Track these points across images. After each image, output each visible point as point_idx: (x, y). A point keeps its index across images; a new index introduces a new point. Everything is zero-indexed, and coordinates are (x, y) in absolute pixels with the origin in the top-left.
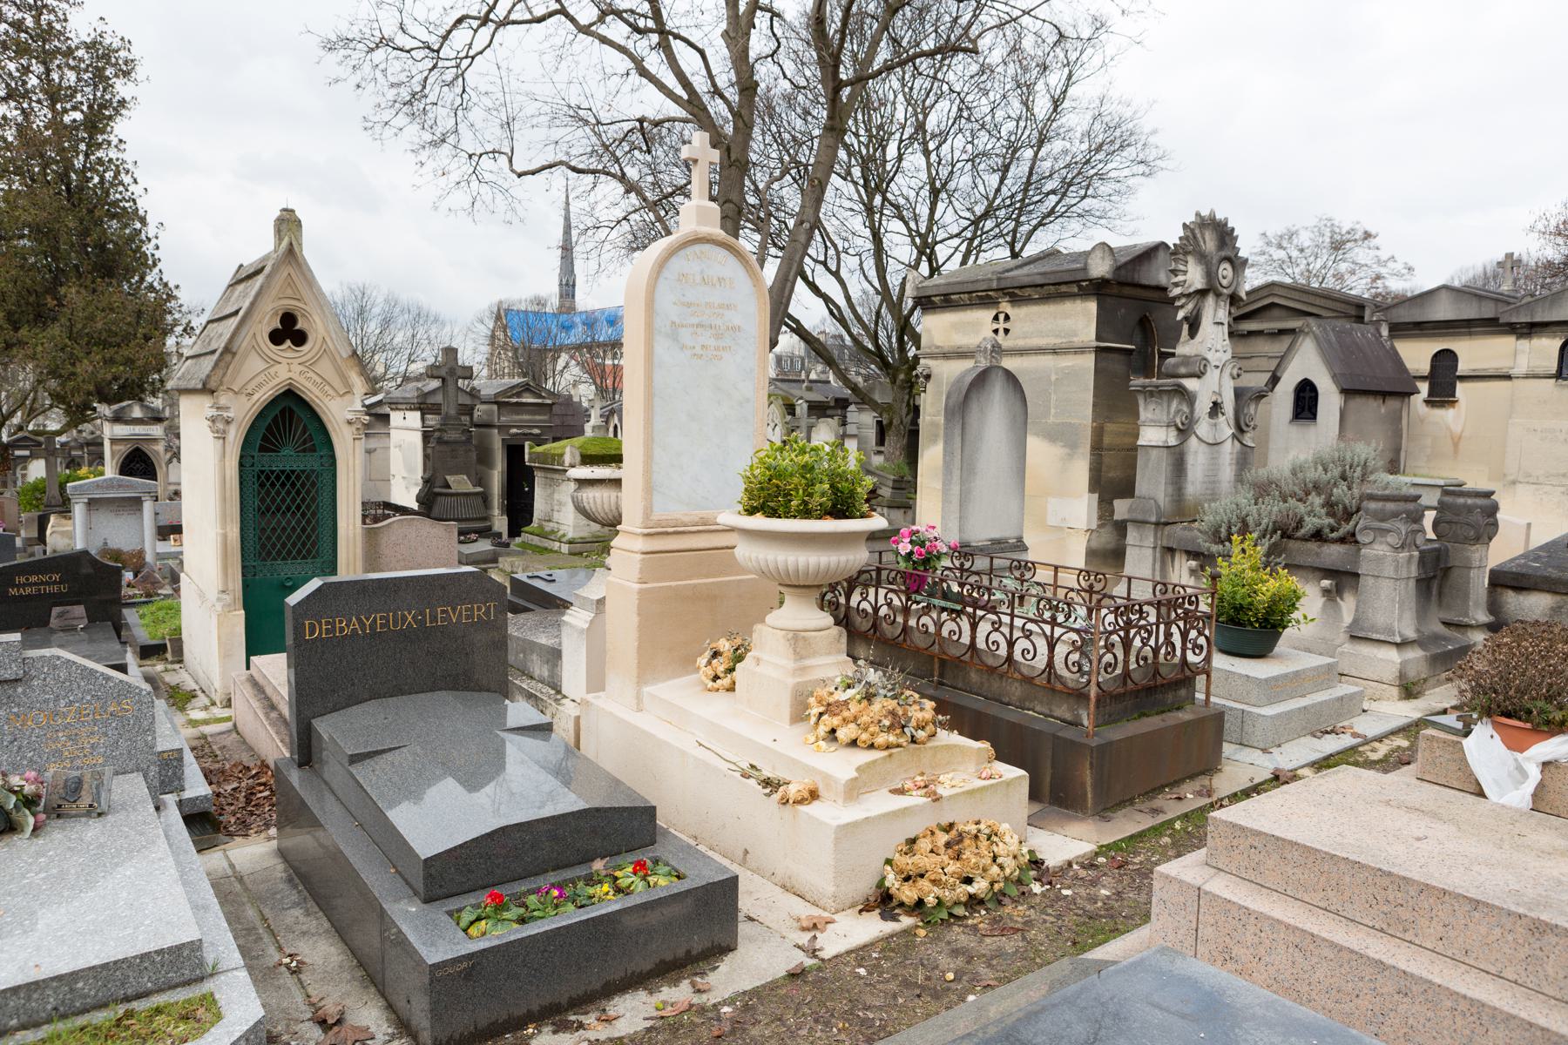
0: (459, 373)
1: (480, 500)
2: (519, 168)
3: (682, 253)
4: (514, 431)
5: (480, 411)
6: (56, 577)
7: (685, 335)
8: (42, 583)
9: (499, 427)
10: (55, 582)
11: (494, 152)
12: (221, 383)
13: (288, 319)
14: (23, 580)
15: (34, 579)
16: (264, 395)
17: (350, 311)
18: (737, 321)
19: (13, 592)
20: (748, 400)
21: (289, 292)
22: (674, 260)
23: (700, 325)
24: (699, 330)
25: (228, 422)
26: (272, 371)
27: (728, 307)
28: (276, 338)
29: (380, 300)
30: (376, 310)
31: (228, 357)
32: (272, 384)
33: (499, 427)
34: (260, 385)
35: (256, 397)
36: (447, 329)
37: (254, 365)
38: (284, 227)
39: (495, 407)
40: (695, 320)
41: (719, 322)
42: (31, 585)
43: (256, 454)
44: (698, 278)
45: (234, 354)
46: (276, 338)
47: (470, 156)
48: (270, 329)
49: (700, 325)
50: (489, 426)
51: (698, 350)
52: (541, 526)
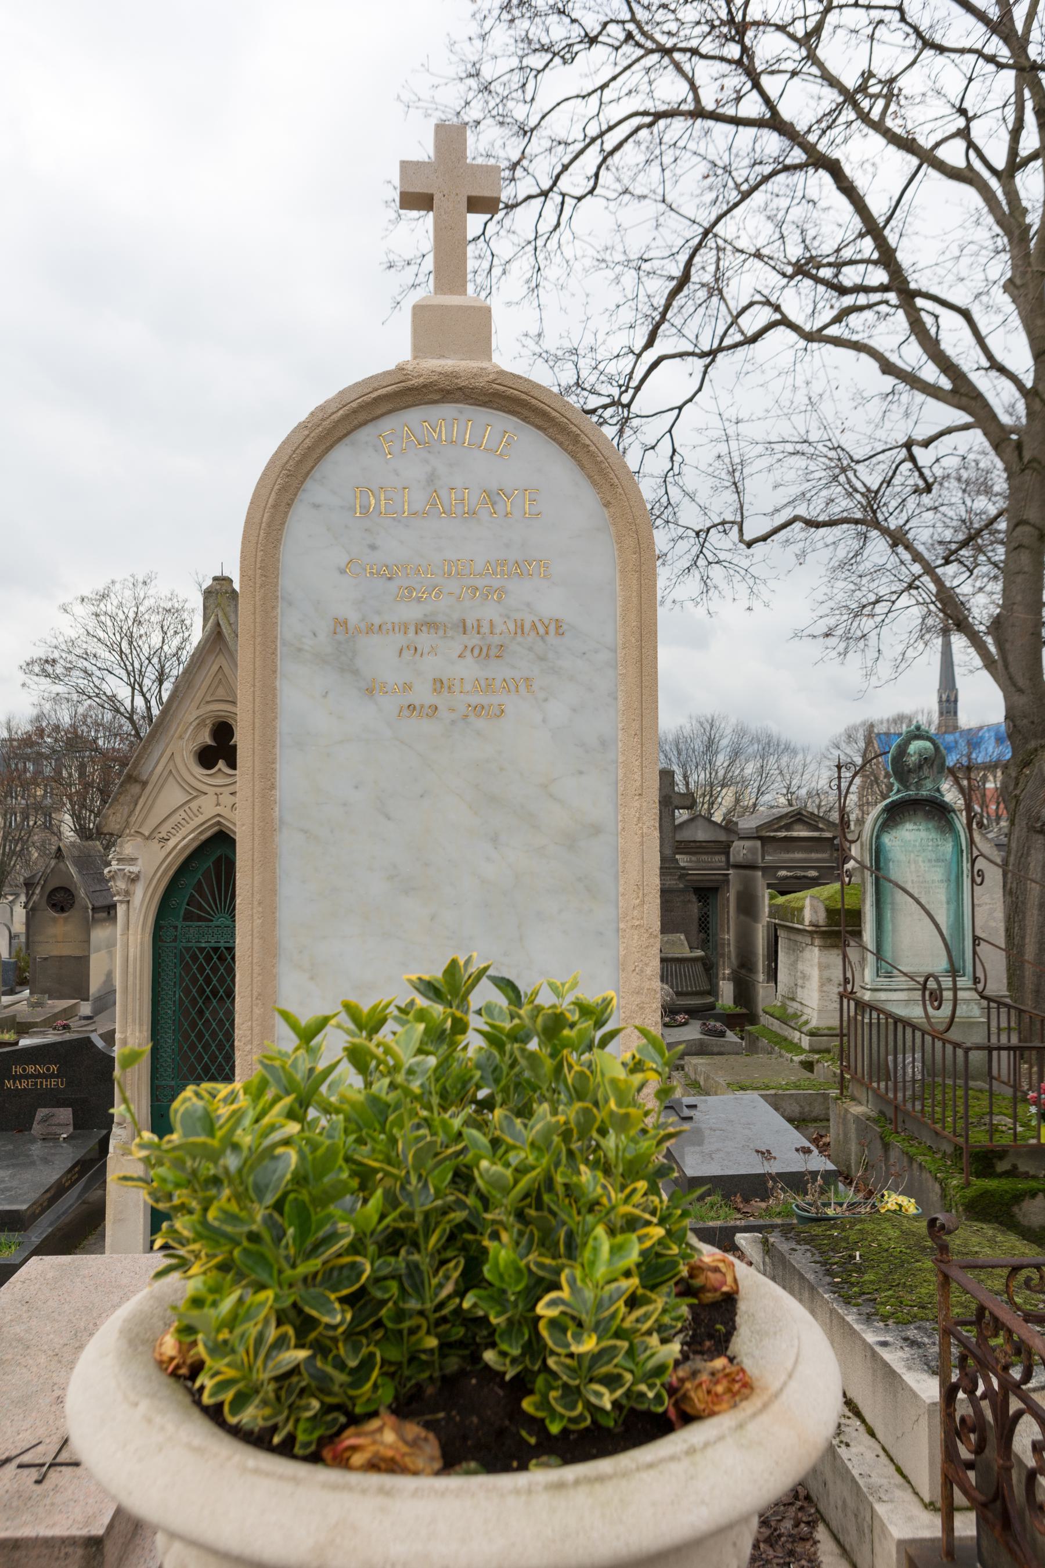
0: (676, 801)
1: (699, 967)
2: (747, 537)
3: (365, 434)
4: (783, 873)
5: (740, 850)
6: (54, 1068)
7: (380, 657)
8: (39, 1076)
9: (764, 869)
10: (52, 1076)
11: (723, 523)
12: (127, 824)
13: (223, 731)
14: (19, 1070)
15: (31, 1069)
16: (183, 839)
17: (699, 745)
18: (551, 603)
19: (8, 1084)
20: (596, 830)
21: (221, 693)
22: (341, 454)
23: (428, 624)
24: (425, 640)
25: (134, 879)
26: (194, 805)
27: (521, 569)
28: (207, 758)
29: (728, 731)
30: (724, 742)
31: (135, 789)
32: (193, 824)
33: (764, 869)
34: (177, 826)
35: (171, 843)
36: (800, 757)
37: (172, 796)
38: (211, 600)
39: (759, 843)
40: (412, 612)
41: (490, 612)
42: (27, 1077)
43: (179, 924)
44: (418, 499)
45: (145, 784)
46: (207, 758)
47: (698, 534)
48: (194, 746)
49: (428, 624)
50: (752, 867)
51: (423, 695)
52: (784, 1006)
